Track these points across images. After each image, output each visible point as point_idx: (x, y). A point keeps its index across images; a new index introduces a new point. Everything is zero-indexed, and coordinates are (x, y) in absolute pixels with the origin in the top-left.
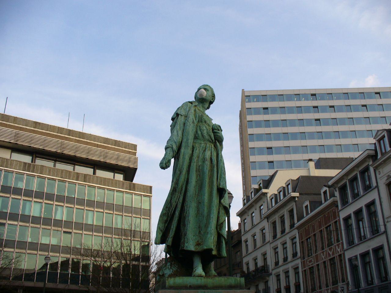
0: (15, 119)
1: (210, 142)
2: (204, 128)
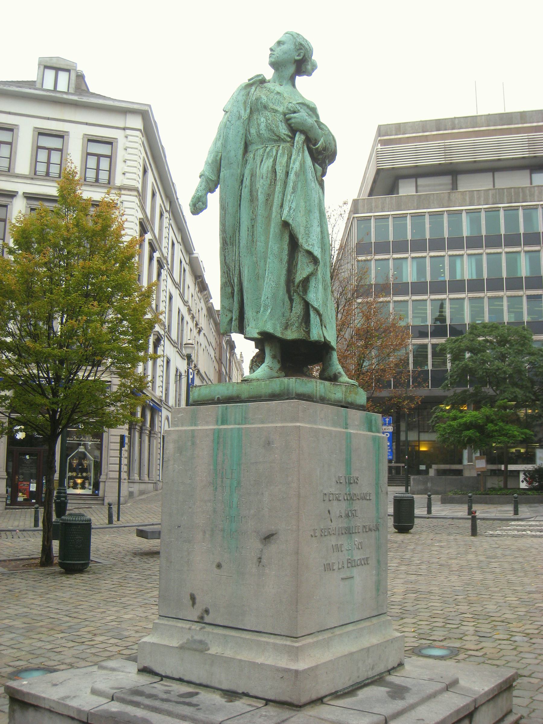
0: (523, 116)
1: (275, 141)
2: (263, 119)
